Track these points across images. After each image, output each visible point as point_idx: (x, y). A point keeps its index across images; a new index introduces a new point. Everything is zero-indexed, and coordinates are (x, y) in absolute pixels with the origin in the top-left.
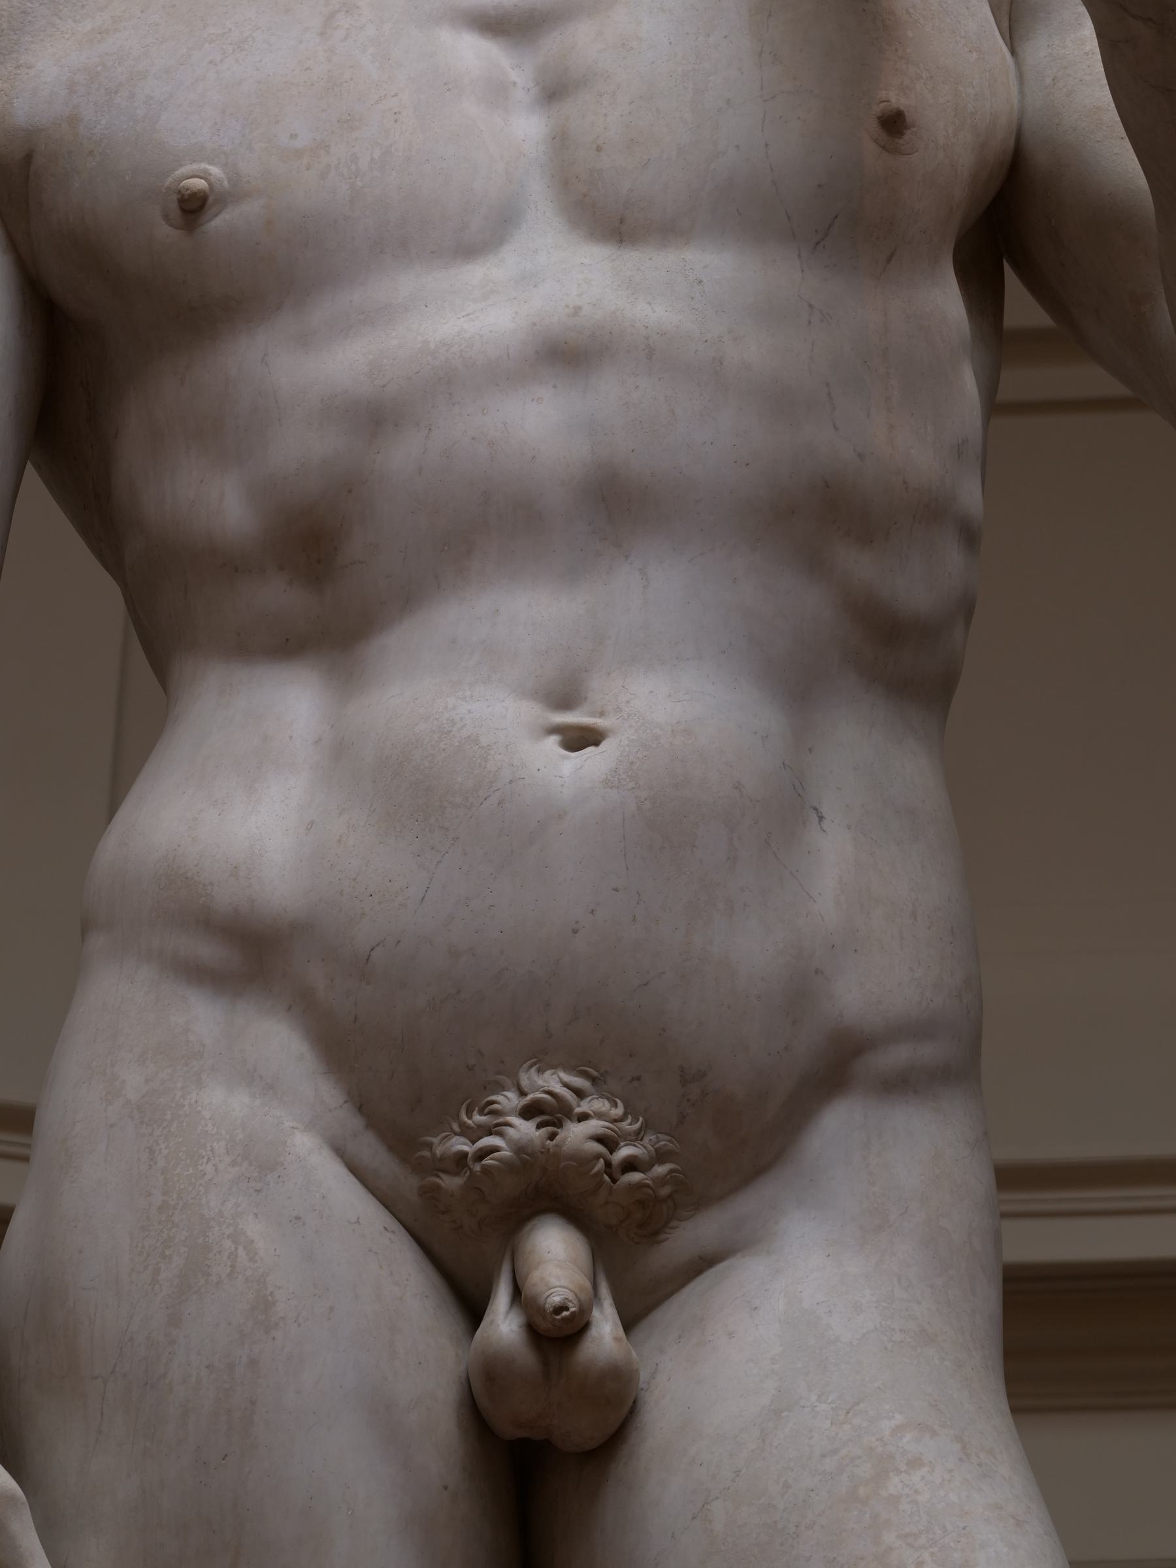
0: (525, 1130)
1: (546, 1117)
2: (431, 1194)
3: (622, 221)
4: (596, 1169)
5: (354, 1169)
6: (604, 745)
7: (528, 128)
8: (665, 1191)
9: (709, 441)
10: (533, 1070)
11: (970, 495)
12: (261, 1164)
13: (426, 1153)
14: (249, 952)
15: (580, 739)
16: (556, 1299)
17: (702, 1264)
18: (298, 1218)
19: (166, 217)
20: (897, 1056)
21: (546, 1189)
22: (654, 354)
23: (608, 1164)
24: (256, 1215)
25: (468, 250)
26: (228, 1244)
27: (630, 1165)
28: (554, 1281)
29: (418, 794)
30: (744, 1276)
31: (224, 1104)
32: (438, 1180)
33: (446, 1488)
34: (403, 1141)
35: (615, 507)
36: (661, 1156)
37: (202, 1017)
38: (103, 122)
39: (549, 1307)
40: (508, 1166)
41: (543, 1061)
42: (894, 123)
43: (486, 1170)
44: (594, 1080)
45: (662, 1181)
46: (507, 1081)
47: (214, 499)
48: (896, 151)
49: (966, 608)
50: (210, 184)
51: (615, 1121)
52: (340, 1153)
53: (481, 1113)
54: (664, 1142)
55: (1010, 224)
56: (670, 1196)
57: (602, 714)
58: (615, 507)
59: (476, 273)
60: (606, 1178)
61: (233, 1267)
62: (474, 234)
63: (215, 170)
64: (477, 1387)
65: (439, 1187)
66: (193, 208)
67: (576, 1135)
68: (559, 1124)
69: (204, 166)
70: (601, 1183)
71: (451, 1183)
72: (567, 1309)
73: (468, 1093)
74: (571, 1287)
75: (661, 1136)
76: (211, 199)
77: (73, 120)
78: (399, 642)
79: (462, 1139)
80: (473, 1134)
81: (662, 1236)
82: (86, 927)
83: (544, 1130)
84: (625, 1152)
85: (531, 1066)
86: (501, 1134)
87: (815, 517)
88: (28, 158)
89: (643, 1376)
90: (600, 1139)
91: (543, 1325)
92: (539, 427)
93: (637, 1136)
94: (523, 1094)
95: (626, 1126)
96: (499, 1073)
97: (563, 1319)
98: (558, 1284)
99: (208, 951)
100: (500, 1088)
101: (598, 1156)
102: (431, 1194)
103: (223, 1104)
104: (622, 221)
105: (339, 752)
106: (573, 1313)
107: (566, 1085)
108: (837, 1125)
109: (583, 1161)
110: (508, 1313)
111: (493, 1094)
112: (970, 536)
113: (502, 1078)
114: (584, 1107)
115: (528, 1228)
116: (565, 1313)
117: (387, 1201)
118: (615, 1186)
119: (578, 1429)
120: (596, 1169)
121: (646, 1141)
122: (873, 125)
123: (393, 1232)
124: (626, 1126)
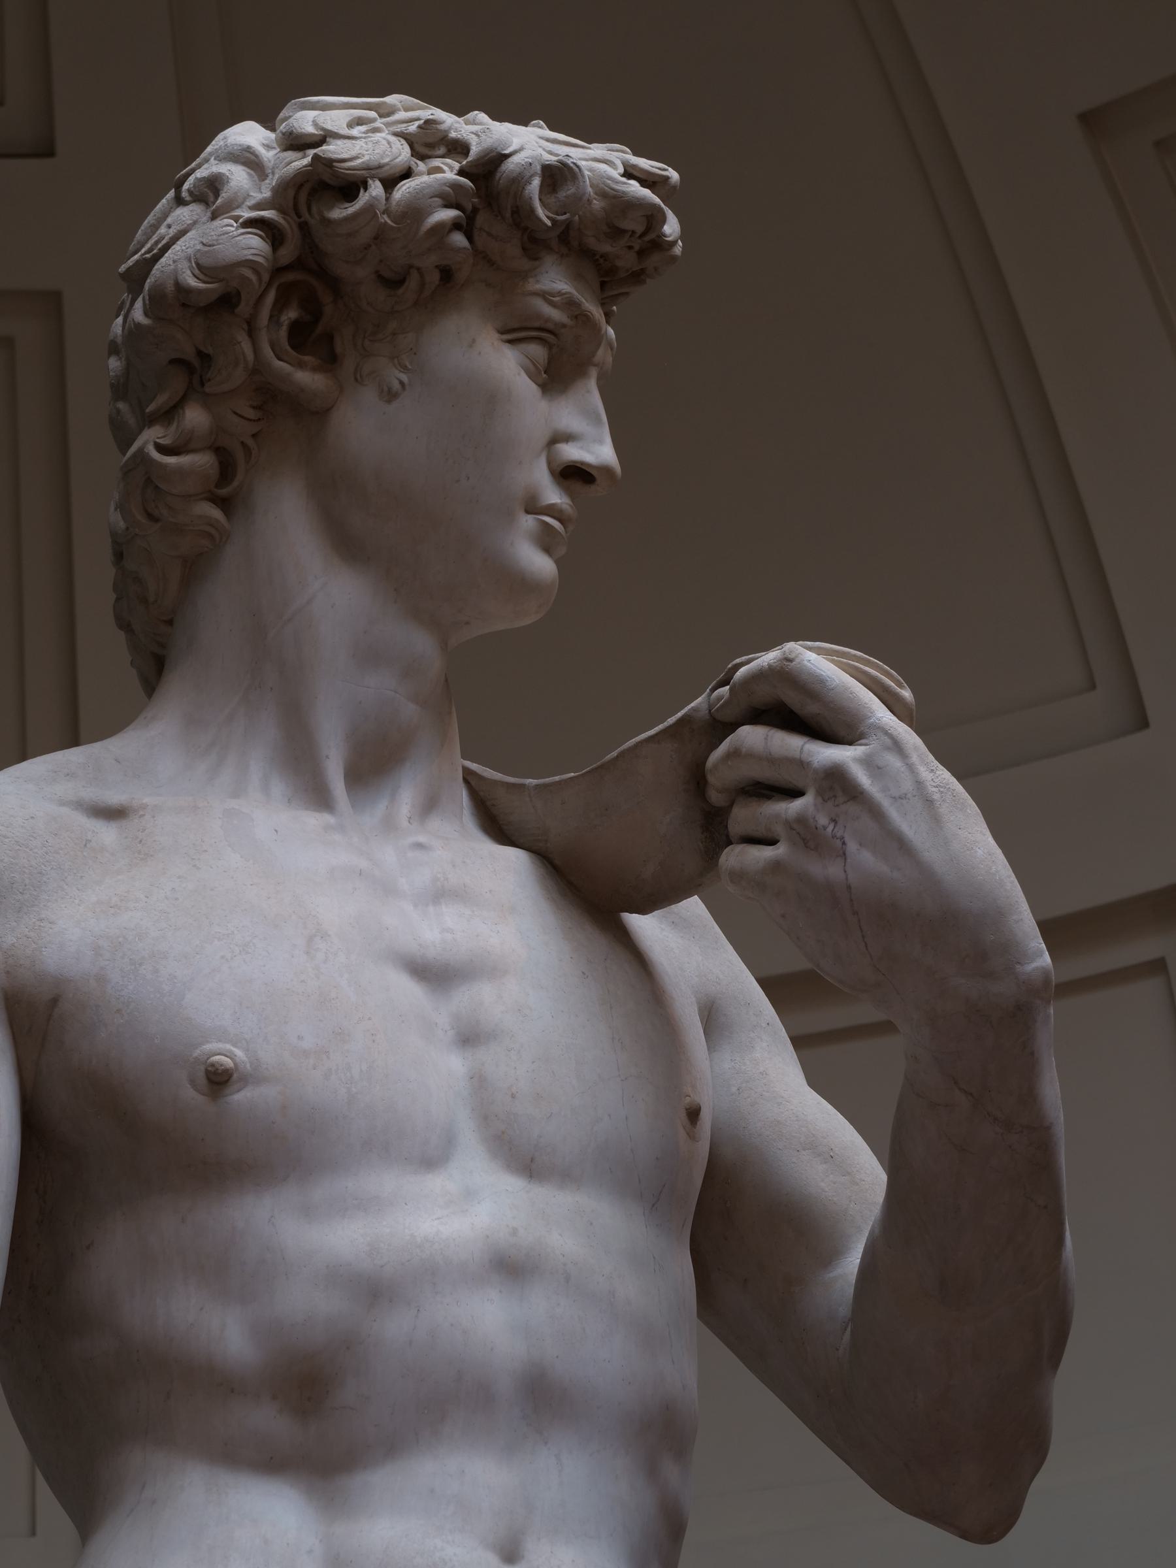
3: (532, 1160)
7: (455, 1065)
9: (604, 1359)
19: (192, 1082)
25: (431, 1160)
35: (541, 1401)
38: (131, 987)
50: (235, 1064)
58: (541, 1401)
59: (437, 1183)
63: (239, 1053)
66: (218, 1080)
69: (229, 1047)
76: (235, 1075)
77: (101, 979)
78: (380, 1480)
87: (660, 1436)
88: (55, 1001)
92: (491, 1325)
104: (532, 1160)
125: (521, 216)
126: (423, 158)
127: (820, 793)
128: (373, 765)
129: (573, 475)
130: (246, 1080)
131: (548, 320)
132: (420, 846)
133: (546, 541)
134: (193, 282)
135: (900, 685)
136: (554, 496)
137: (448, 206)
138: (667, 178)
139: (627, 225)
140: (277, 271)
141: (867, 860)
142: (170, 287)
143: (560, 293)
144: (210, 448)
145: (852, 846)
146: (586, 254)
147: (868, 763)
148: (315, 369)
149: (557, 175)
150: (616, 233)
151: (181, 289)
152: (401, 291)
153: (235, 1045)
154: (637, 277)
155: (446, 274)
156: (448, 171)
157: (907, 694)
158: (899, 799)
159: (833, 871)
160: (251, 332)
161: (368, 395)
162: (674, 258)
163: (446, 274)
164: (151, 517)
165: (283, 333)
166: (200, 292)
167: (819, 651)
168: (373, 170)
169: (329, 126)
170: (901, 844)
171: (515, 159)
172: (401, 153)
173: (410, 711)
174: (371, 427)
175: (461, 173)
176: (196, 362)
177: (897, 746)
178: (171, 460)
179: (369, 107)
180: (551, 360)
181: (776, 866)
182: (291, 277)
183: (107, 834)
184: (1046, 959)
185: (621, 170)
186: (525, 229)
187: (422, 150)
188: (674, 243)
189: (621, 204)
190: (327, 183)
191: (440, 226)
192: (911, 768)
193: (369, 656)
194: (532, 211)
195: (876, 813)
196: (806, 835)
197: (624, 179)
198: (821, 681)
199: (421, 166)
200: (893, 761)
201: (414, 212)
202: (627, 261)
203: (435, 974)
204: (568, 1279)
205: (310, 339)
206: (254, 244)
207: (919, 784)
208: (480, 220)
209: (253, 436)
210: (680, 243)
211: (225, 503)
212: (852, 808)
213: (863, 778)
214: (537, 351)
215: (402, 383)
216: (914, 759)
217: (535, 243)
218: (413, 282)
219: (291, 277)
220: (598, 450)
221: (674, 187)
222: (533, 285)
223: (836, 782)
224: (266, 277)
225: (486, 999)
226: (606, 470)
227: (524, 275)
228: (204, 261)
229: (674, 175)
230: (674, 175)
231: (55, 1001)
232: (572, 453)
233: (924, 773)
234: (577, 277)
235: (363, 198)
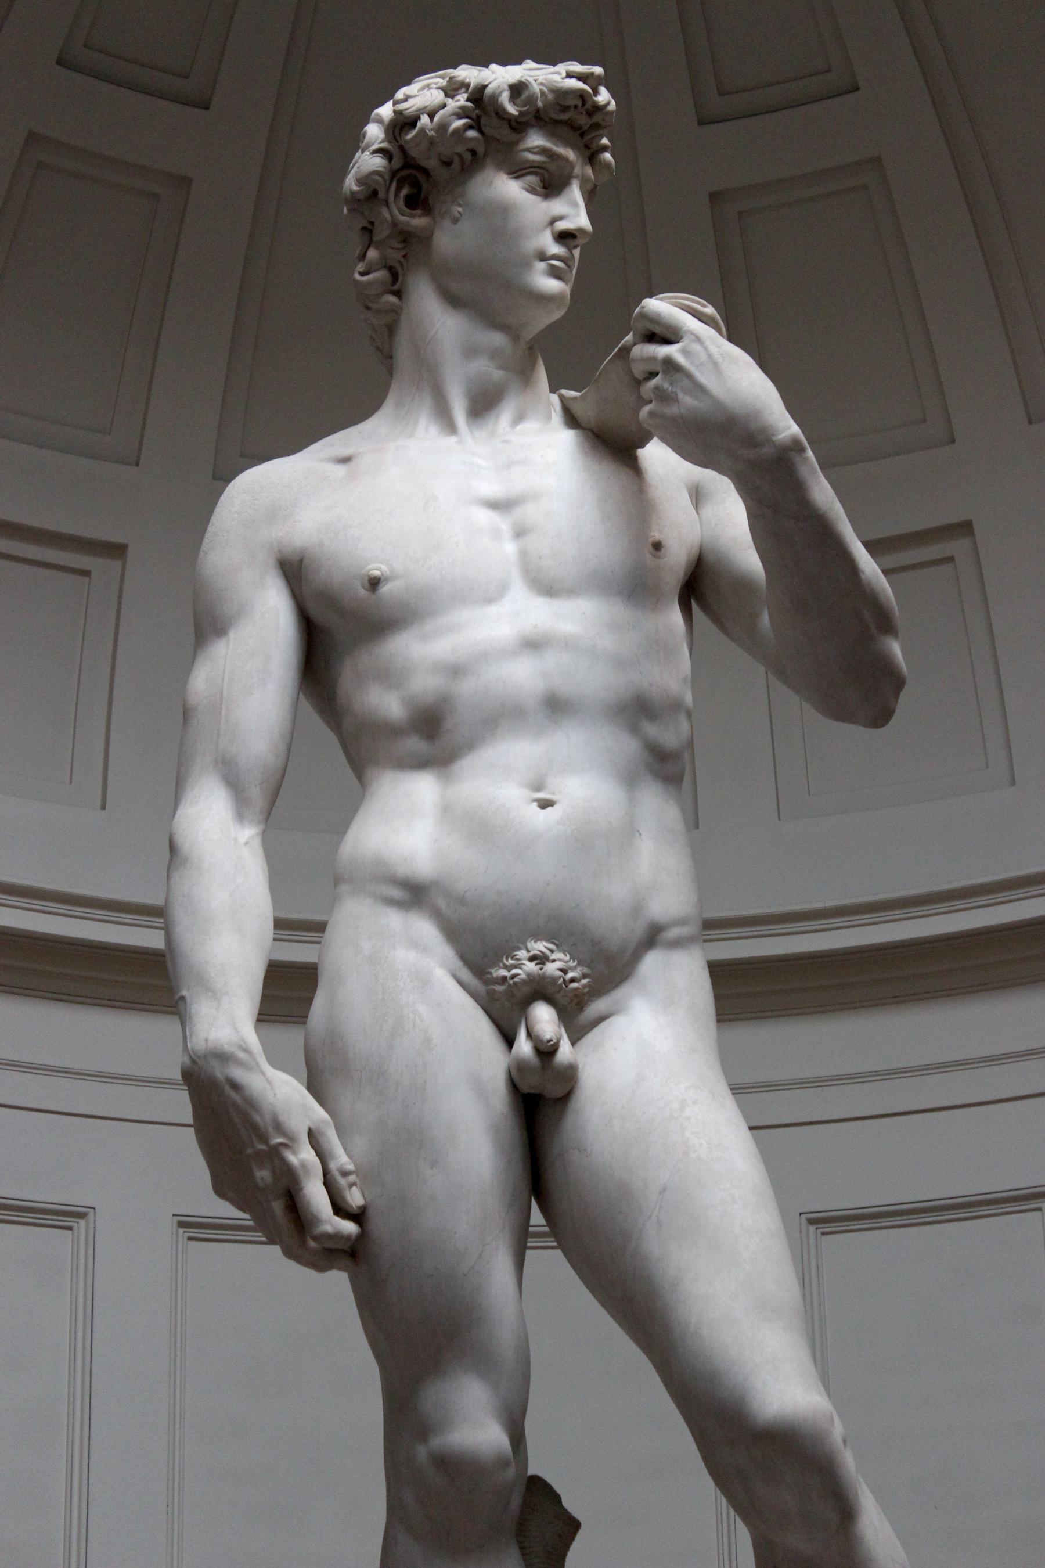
0: (531, 967)
2: (491, 994)
6: (555, 806)
7: (510, 548)
8: (586, 990)
9: (594, 681)
11: (689, 699)
12: (423, 981)
13: (489, 976)
14: (414, 894)
15: (545, 804)
16: (548, 1037)
17: (601, 1019)
19: (364, 587)
20: (673, 933)
21: (540, 990)
22: (568, 644)
25: (489, 600)
26: (411, 1015)
27: (573, 980)
29: (479, 827)
30: (616, 1025)
31: (404, 956)
35: (556, 707)
36: (584, 976)
37: (395, 920)
40: (524, 981)
41: (537, 938)
42: (657, 546)
43: (515, 984)
44: (557, 946)
45: (584, 986)
47: (388, 704)
48: (659, 557)
49: (690, 743)
53: (512, 959)
54: (586, 970)
55: (700, 585)
57: (554, 794)
58: (556, 707)
59: (493, 610)
62: (493, 595)
63: (384, 567)
64: (513, 1072)
65: (494, 990)
66: (374, 583)
67: (551, 968)
68: (544, 964)
73: (504, 950)
80: (508, 968)
82: (337, 881)
83: (539, 966)
84: (570, 975)
88: (301, 560)
89: (581, 1066)
90: (561, 970)
91: (542, 1048)
92: (523, 676)
93: (573, 969)
94: (528, 951)
99: (396, 893)
100: (519, 949)
101: (560, 977)
102: (491, 994)
103: (404, 956)
105: (446, 811)
108: (651, 962)
109: (554, 980)
112: (689, 715)
114: (553, 956)
115: (531, 1007)
119: (554, 1090)
122: (650, 547)
124: (572, 964)
125: (500, 113)
126: (452, 97)
127: (664, 372)
128: (483, 404)
129: (564, 237)
130: (387, 579)
131: (533, 161)
132: (505, 441)
133: (555, 273)
134: (355, 188)
135: (704, 306)
136: (555, 249)
137: (461, 118)
138: (592, 74)
139: (572, 102)
140: (393, 174)
141: (688, 401)
142: (348, 193)
143: (537, 147)
144: (385, 267)
145: (681, 395)
146: (556, 122)
147: (685, 352)
148: (420, 216)
149: (517, 89)
150: (565, 109)
151: (353, 193)
152: (452, 167)
153: (382, 563)
154: (597, 126)
155: (473, 152)
156: (462, 99)
157: (710, 310)
158: (700, 366)
159: (672, 410)
160: (388, 206)
161: (447, 223)
162: (611, 113)
163: (473, 152)
164: (368, 308)
165: (401, 202)
166: (358, 192)
167: (661, 299)
168: (422, 111)
169: (408, 93)
170: (700, 389)
171: (490, 86)
172: (438, 97)
173: (498, 375)
174: (452, 238)
175: (468, 100)
176: (370, 227)
177: (698, 339)
178: (365, 278)
179: (436, 77)
180: (543, 180)
181: (652, 414)
182: (404, 173)
183: (341, 470)
184: (794, 429)
185: (564, 75)
186: (503, 119)
187: (450, 93)
188: (608, 103)
189: (561, 94)
190: (403, 123)
191: (457, 132)
192: (705, 348)
193: (471, 352)
194: (504, 110)
195: (689, 376)
196: (663, 396)
197: (568, 80)
198: (659, 315)
199: (449, 101)
200: (696, 347)
201: (443, 127)
202: (583, 121)
203: (499, 505)
204: (567, 644)
205: (416, 202)
206: (378, 162)
207: (710, 356)
208: (483, 121)
209: (404, 256)
210: (613, 103)
211: (398, 294)
212: (678, 376)
213: (681, 359)
214: (532, 179)
215: (460, 213)
216: (708, 343)
217: (518, 126)
218: (456, 160)
219: (404, 173)
220: (579, 219)
221: (599, 76)
222: (522, 146)
223: (669, 364)
224: (387, 177)
225: (530, 512)
226: (582, 231)
227: (518, 142)
228: (359, 176)
229: (598, 70)
230: (598, 70)
231: (301, 560)
232: (562, 225)
233: (713, 349)
234: (552, 135)
235: (419, 124)
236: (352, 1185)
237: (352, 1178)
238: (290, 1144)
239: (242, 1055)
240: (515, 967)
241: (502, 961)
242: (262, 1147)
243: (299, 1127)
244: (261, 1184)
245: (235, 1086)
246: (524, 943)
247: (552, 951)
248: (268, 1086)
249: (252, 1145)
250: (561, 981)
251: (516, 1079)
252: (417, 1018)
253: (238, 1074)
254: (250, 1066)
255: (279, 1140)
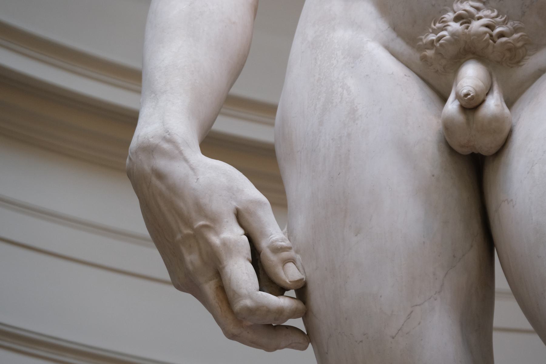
0: (455, 26)
1: (464, 20)
2: (424, 59)
4: (485, 38)
5: (394, 54)
8: (519, 44)
10: (459, 2)
12: (354, 56)
13: (420, 43)
16: (465, 91)
18: (367, 75)
21: (467, 50)
23: (491, 36)
24: (352, 77)
26: (340, 89)
27: (501, 35)
28: (465, 84)
32: (425, 53)
33: (433, 176)
34: (411, 40)
39: (462, 95)
43: (441, 45)
44: (484, 3)
45: (518, 40)
46: (449, 9)
51: (493, 18)
52: (387, 48)
53: (439, 23)
54: (517, 24)
56: (523, 46)
60: (491, 41)
61: (342, 98)
67: (476, 26)
68: (469, 22)
70: (488, 44)
71: (430, 53)
72: (469, 94)
74: (471, 85)
75: (515, 22)
79: (433, 35)
80: (435, 32)
81: (522, 63)
83: (463, 26)
84: (498, 30)
85: (457, 1)
86: (446, 30)
90: (487, 26)
93: (504, 23)
94: (455, 12)
95: (498, 19)
96: (445, 6)
97: (468, 99)
98: (466, 85)
100: (446, 12)
101: (485, 33)
102: (424, 59)
103: (342, 35)
106: (473, 97)
107: (472, 6)
109: (480, 35)
110: (453, 101)
111: (444, 14)
113: (446, 7)
114: (480, 14)
116: (469, 96)
117: (408, 64)
118: (495, 44)
119: (486, 145)
120: (485, 38)
121: (509, 25)
123: (409, 76)
236: (285, 261)
237: (285, 255)
238: (212, 225)
239: (166, 146)
240: (443, 29)
241: (430, 26)
242: (187, 231)
243: (223, 207)
244: (190, 267)
245: (160, 176)
246: (451, 6)
247: (478, 9)
248: (191, 172)
249: (181, 232)
250: (487, 36)
251: (448, 140)
252: (345, 92)
253: (162, 164)
254: (178, 154)
255: (202, 223)
